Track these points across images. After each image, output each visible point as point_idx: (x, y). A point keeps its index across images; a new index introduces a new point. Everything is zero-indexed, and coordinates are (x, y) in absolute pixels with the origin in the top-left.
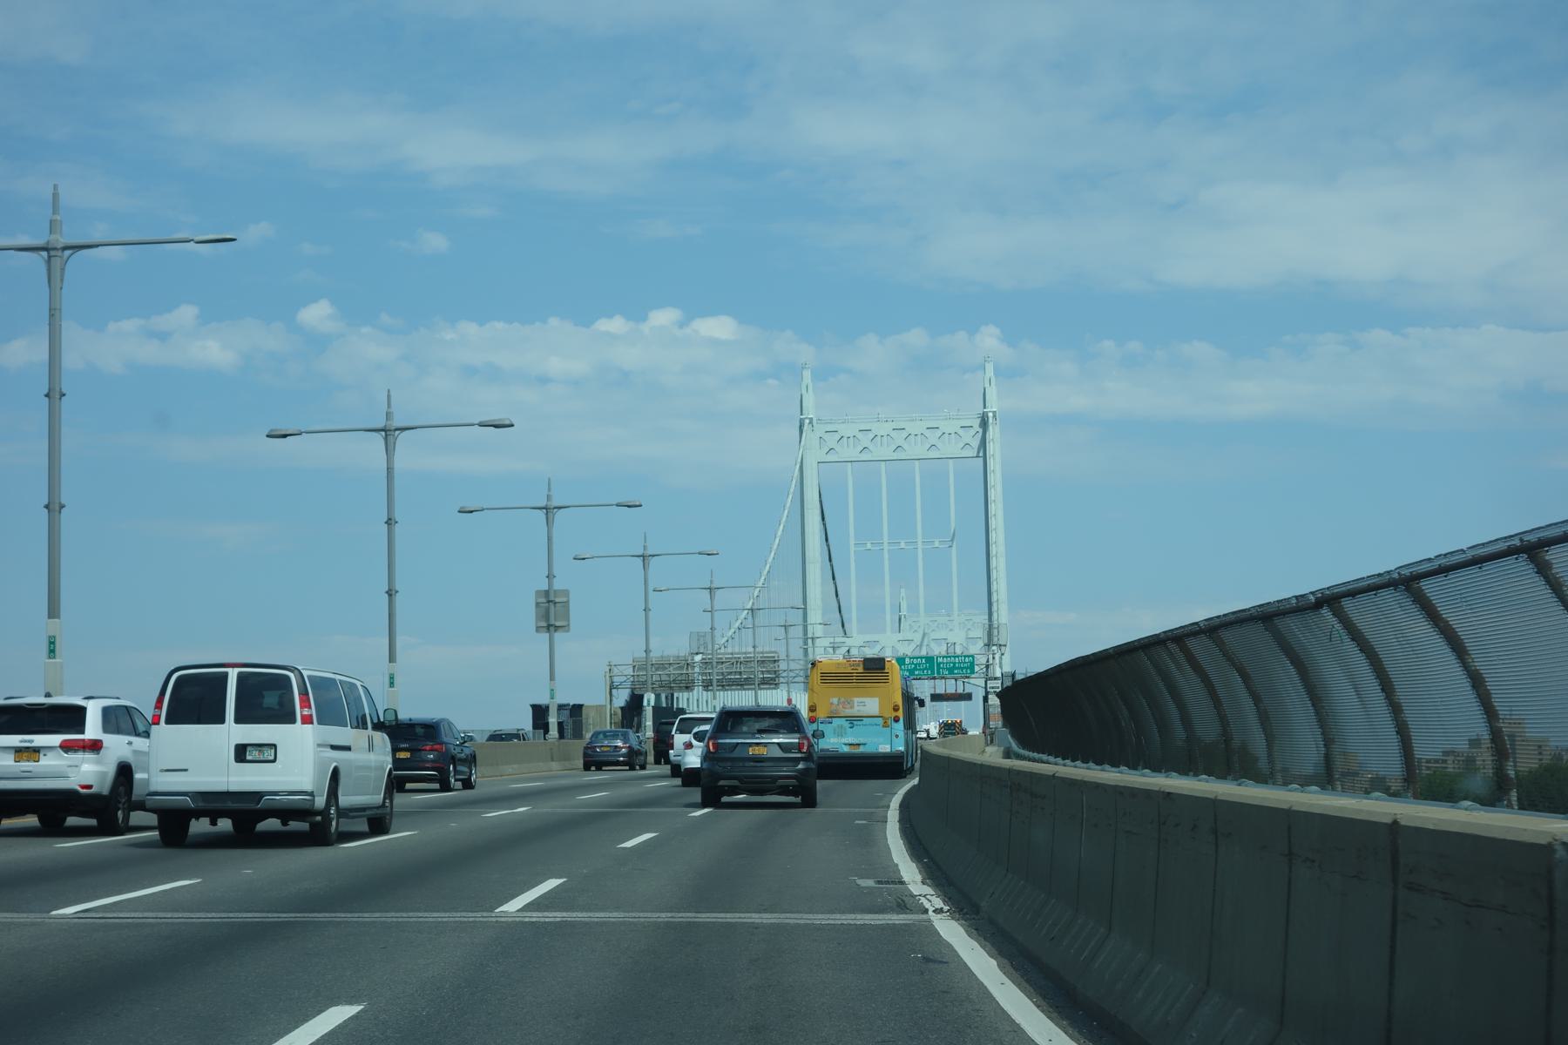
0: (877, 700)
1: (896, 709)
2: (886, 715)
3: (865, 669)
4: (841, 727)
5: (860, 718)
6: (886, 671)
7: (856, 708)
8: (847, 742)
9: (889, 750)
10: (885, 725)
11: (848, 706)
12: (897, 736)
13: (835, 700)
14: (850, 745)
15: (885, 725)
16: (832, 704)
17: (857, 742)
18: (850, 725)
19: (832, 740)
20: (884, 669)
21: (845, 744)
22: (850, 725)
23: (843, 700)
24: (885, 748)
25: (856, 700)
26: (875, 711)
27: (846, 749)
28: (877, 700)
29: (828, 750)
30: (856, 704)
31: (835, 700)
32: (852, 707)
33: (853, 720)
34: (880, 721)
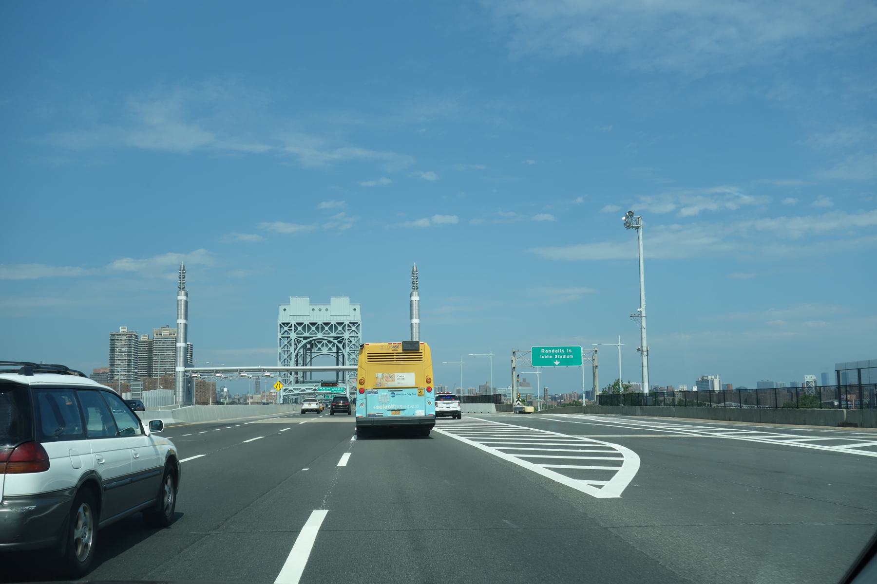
0: (413, 374)
1: (429, 381)
2: (421, 386)
3: (403, 350)
4: (385, 396)
5: (400, 389)
6: (420, 352)
7: (397, 381)
8: (389, 408)
9: (423, 414)
10: (420, 394)
11: (391, 379)
12: (429, 403)
13: (380, 375)
14: (392, 410)
15: (420, 394)
16: (377, 378)
17: (398, 408)
18: (392, 395)
19: (378, 407)
20: (419, 350)
21: (388, 410)
22: (392, 395)
23: (385, 374)
24: (420, 413)
25: (396, 374)
26: (412, 383)
27: (390, 414)
28: (413, 374)
29: (374, 415)
30: (396, 378)
31: (380, 375)
32: (393, 380)
33: (394, 390)
34: (416, 391)
